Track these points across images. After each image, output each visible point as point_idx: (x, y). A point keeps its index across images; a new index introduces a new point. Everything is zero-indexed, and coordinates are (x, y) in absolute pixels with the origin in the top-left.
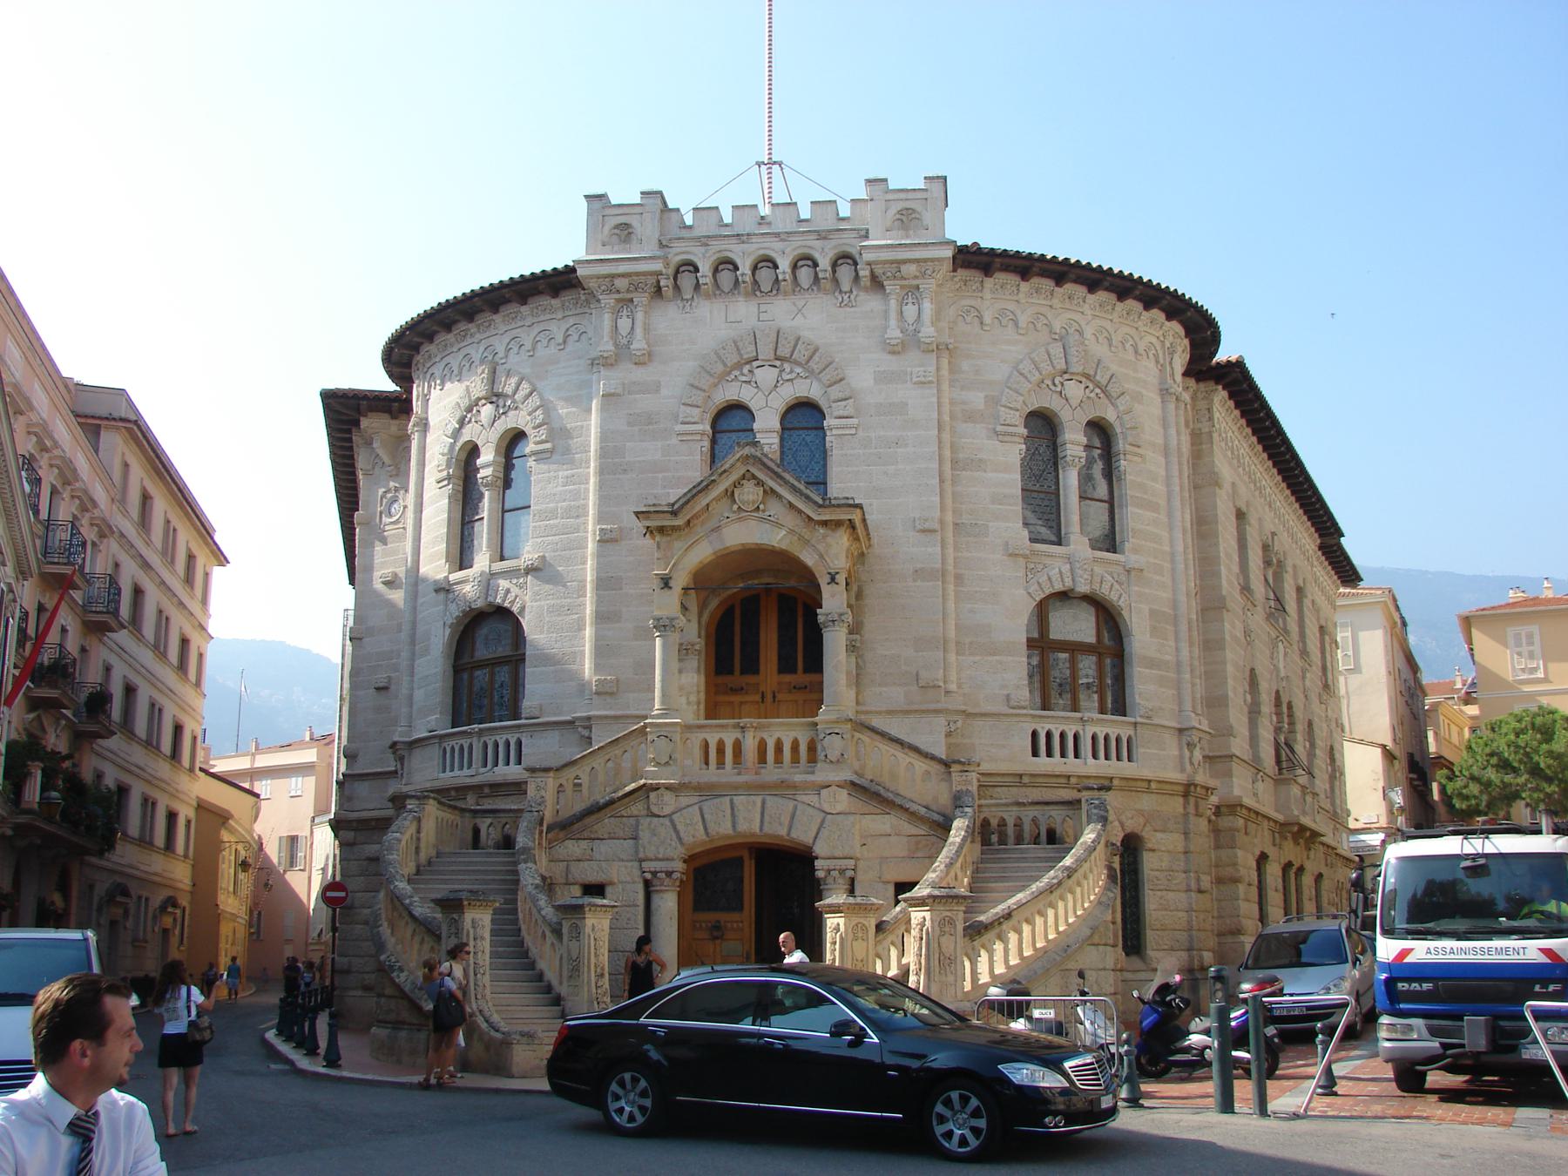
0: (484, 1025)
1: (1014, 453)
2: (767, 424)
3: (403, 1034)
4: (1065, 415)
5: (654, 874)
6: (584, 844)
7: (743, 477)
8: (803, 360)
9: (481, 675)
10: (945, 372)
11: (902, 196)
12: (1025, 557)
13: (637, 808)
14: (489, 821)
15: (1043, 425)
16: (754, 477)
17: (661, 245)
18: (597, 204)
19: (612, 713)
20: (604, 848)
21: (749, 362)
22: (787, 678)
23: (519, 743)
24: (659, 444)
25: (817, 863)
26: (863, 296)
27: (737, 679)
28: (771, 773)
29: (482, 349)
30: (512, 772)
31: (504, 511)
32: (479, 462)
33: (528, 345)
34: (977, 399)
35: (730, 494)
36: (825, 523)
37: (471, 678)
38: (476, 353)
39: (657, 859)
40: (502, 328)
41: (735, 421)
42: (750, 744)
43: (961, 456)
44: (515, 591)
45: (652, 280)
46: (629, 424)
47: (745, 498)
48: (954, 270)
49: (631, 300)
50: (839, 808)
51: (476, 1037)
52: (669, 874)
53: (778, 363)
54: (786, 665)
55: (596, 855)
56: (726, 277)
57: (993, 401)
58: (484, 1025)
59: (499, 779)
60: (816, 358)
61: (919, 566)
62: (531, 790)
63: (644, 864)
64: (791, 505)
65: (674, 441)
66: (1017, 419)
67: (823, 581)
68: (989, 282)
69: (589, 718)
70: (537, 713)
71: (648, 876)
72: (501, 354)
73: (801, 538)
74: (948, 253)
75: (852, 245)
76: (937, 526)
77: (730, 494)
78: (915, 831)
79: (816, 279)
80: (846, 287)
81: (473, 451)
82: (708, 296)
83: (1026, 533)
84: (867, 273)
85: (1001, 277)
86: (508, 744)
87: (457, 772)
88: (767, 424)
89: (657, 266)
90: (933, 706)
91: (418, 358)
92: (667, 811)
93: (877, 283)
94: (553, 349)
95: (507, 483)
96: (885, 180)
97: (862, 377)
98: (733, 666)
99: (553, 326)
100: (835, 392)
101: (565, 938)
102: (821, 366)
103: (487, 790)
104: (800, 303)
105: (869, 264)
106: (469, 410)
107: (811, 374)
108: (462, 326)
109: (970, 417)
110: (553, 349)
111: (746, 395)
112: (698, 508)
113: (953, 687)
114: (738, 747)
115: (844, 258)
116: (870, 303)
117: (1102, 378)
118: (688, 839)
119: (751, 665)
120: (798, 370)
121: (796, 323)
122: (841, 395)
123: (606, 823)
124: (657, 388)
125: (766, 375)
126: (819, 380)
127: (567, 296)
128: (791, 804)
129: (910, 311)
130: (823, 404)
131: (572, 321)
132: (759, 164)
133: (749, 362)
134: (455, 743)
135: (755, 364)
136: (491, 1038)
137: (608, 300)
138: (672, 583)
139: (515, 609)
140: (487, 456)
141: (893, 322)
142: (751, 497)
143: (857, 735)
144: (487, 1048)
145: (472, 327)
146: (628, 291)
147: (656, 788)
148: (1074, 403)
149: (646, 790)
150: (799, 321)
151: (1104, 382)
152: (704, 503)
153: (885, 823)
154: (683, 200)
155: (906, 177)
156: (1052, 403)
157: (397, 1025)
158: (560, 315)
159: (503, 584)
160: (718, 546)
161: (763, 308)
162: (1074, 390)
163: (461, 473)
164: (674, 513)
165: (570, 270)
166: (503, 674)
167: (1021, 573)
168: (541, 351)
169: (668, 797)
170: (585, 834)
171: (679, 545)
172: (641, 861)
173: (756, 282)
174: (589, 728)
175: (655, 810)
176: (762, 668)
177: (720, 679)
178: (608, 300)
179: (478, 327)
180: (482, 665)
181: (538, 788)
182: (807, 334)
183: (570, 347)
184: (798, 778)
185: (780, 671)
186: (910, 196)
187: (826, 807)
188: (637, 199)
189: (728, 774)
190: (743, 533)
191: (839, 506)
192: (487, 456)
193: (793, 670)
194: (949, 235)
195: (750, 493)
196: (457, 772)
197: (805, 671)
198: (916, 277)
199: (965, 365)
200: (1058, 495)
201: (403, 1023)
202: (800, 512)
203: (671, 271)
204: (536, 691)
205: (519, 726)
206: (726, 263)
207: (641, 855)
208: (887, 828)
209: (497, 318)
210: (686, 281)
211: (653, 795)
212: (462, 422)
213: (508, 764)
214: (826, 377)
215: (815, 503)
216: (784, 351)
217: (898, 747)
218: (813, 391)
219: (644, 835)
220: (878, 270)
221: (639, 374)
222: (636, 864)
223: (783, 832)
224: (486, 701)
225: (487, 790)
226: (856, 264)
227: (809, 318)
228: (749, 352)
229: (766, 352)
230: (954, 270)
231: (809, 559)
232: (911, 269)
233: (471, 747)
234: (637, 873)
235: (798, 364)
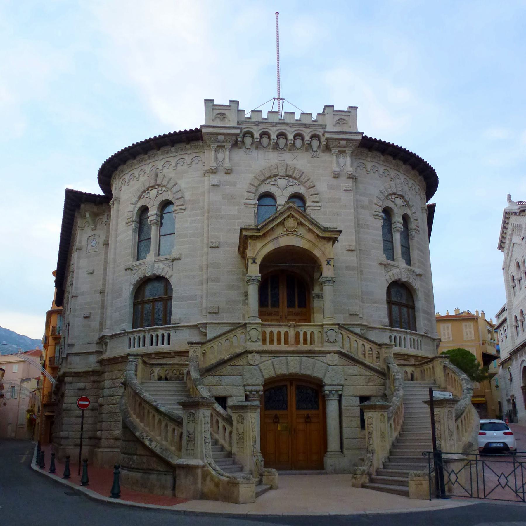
0: (214, 473)
1: (380, 223)
2: (281, 201)
3: (153, 477)
4: (396, 210)
5: (251, 392)
6: (217, 378)
7: (288, 216)
8: (297, 177)
9: (148, 307)
10: (354, 188)
11: (340, 113)
12: (385, 265)
13: (241, 361)
14: (159, 369)
15: (387, 212)
16: (293, 216)
17: (239, 124)
18: (211, 104)
19: (215, 321)
20: (226, 380)
21: (275, 176)
22: (291, 310)
23: (169, 335)
24: (237, 207)
25: (326, 388)
26: (322, 154)
27: (270, 309)
28: (302, 347)
29: (150, 166)
30: (166, 348)
31: (160, 236)
32: (149, 214)
33: (174, 164)
34: (365, 200)
35: (282, 223)
36: (324, 238)
37: (143, 308)
38: (148, 168)
39: (253, 385)
40: (161, 157)
41: (268, 201)
42: (292, 333)
43: (361, 222)
44: (166, 269)
45: (234, 138)
46: (223, 198)
47: (290, 225)
48: (359, 147)
49: (224, 147)
50: (335, 363)
51: (208, 479)
52: (258, 392)
53: (287, 178)
54: (291, 304)
55: (223, 383)
56: (265, 141)
57: (371, 202)
58: (214, 473)
59: (160, 351)
60: (303, 177)
61: (347, 265)
62: (191, 354)
63: (247, 388)
64: (310, 230)
65: (243, 207)
66: (380, 209)
67: (324, 263)
68: (370, 154)
69: (206, 324)
70: (178, 321)
71: (248, 393)
72: (160, 168)
73: (314, 244)
74: (360, 137)
75: (320, 132)
76: (354, 249)
77: (282, 223)
78: (367, 373)
79: (303, 145)
80: (315, 149)
81: (144, 210)
82: (257, 148)
83: (385, 256)
84: (325, 143)
85: (375, 153)
86: (163, 336)
87: (137, 348)
88: (281, 201)
89: (238, 131)
90: (356, 323)
91: (117, 172)
92: (257, 363)
93: (328, 149)
94: (185, 166)
95: (161, 225)
96: (333, 106)
97: (322, 186)
98: (268, 303)
99: (186, 157)
100: (312, 191)
101: (235, 422)
102: (305, 180)
103: (153, 356)
104: (296, 154)
105: (327, 139)
106: (144, 192)
107: (302, 183)
108: (141, 156)
109: (363, 207)
110: (185, 166)
111: (273, 189)
112: (269, 228)
113: (361, 316)
114: (286, 333)
115: (314, 136)
116: (325, 157)
117: (406, 197)
118: (267, 376)
119: (276, 304)
120: (296, 181)
121: (292, 162)
122: (314, 193)
123: (228, 369)
124: (235, 185)
125: (282, 182)
126: (305, 186)
127: (194, 144)
128: (313, 360)
129: (341, 161)
130: (306, 195)
131: (194, 155)
132: (274, 99)
133: (275, 176)
134: (136, 336)
135: (278, 177)
136: (220, 480)
137: (214, 145)
138: (256, 261)
139: (167, 276)
140: (153, 212)
141: (335, 165)
142: (292, 226)
143: (340, 331)
144: (217, 485)
145: (146, 157)
146: (223, 142)
147: (251, 352)
148: (398, 206)
149: (247, 353)
150: (295, 162)
151: (408, 199)
152: (272, 226)
153: (356, 369)
154: (247, 106)
155: (341, 106)
156: (391, 205)
157: (148, 471)
158: (189, 152)
159: (161, 265)
160: (277, 246)
161: (280, 155)
162: (398, 201)
163: (138, 220)
164: (259, 230)
165: (197, 131)
166: (160, 306)
167: (383, 272)
168: (179, 168)
169: (257, 356)
170: (218, 373)
171: (259, 244)
172: (244, 386)
173: (277, 144)
174: (206, 328)
175: (252, 363)
176: (281, 305)
177: (264, 309)
178: (214, 145)
179: (149, 156)
180: (148, 302)
181: (195, 352)
182: (298, 167)
183: (194, 165)
184: (317, 349)
185: (289, 306)
186: (343, 114)
187: (330, 363)
188: (228, 104)
189: (283, 347)
190: (286, 241)
191: (332, 231)
192: (153, 212)
193: (294, 306)
194: (359, 130)
195: (291, 223)
196: (137, 348)
197: (299, 306)
198: (345, 147)
199: (361, 186)
200: (392, 242)
201: (153, 470)
202: (314, 232)
203: (241, 135)
204: (179, 311)
205: (169, 328)
206: (265, 134)
207: (245, 383)
208: (355, 372)
209: (159, 153)
210: (248, 140)
211: (250, 356)
212: (139, 198)
213: (163, 344)
214: (309, 184)
215: (321, 229)
216: (290, 173)
217: (358, 337)
218: (301, 190)
219: (247, 375)
220: (330, 143)
221: (227, 178)
222: (242, 388)
223: (309, 372)
224: (150, 318)
225: (153, 356)
226: (319, 140)
227: (300, 161)
228: (275, 172)
229: (282, 173)
230: (359, 147)
231: (317, 253)
232: (343, 143)
233: (144, 337)
234: (243, 391)
235: (295, 178)
